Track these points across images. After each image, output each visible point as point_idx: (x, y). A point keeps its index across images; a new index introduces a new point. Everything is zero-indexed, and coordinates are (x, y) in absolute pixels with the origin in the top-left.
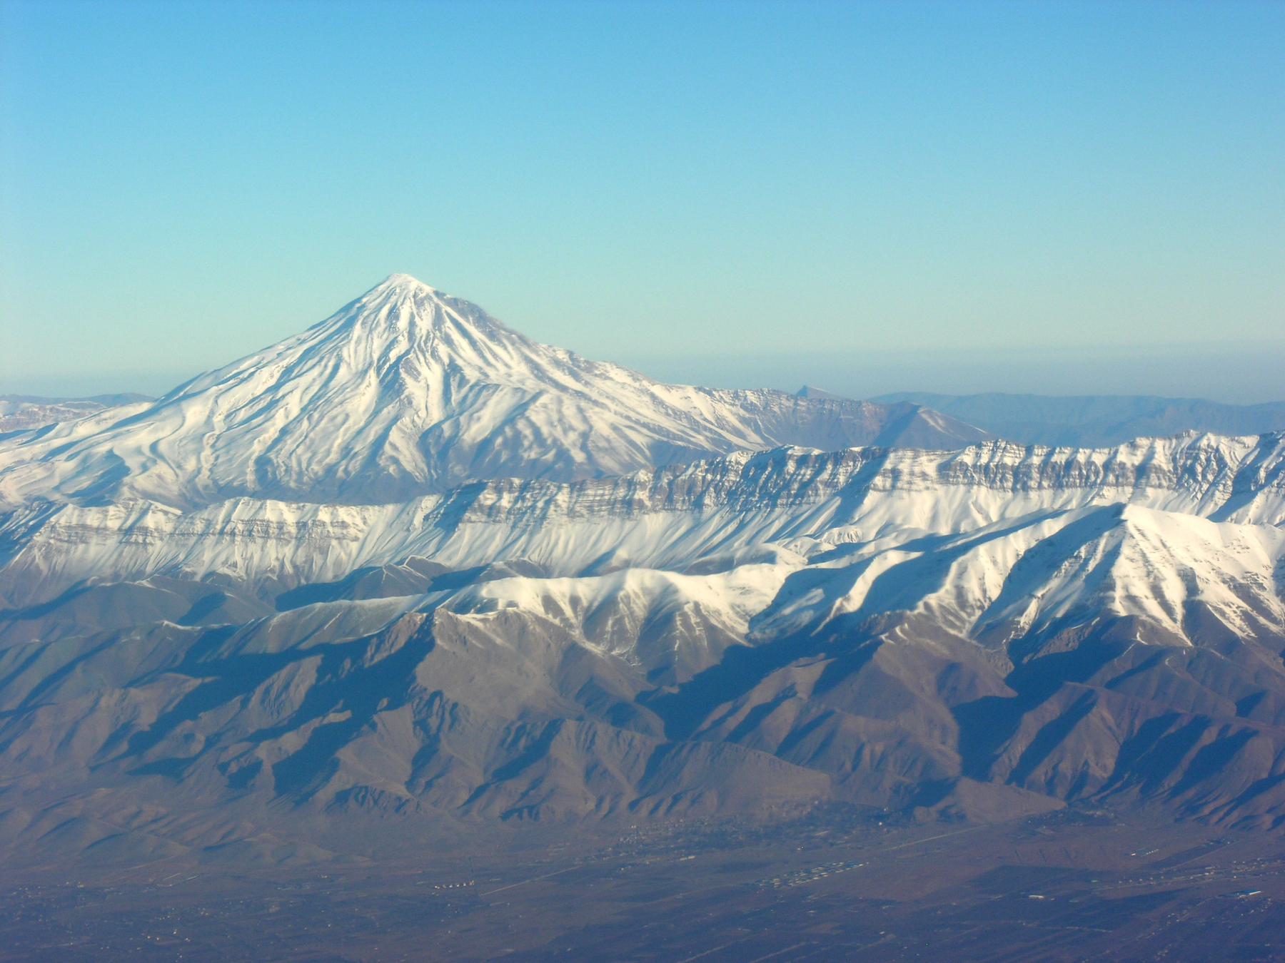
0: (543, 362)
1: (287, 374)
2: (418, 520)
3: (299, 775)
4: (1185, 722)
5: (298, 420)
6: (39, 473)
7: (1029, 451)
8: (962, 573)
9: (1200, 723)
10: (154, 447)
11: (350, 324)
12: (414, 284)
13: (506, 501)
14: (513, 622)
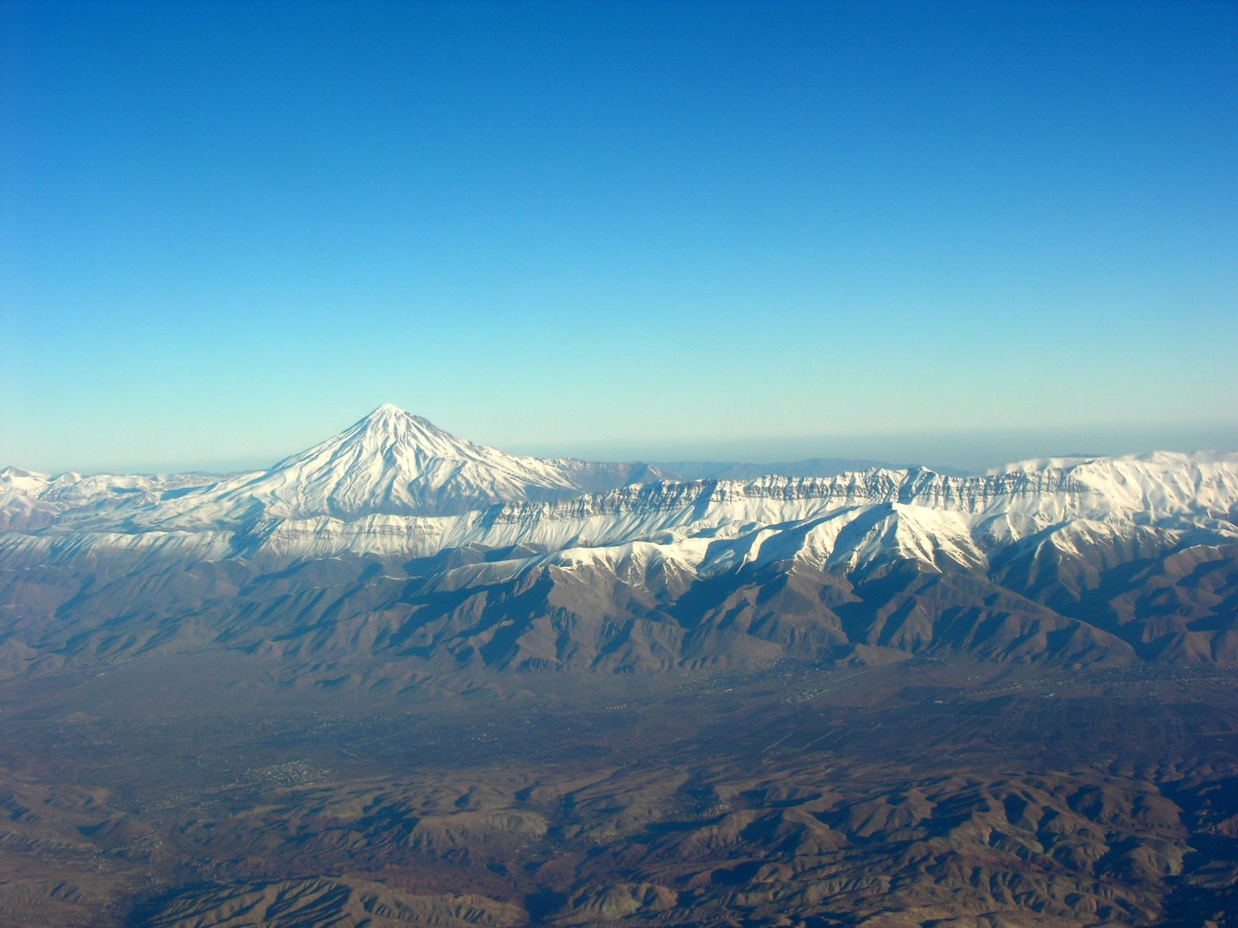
0: (462, 447)
1: (335, 455)
2: (469, 523)
3: (499, 651)
4: (966, 610)
5: (344, 478)
6: (215, 508)
7: (790, 480)
8: (812, 540)
9: (975, 611)
10: (273, 493)
11: (365, 429)
12: (394, 409)
13: (516, 512)
14: (582, 568)
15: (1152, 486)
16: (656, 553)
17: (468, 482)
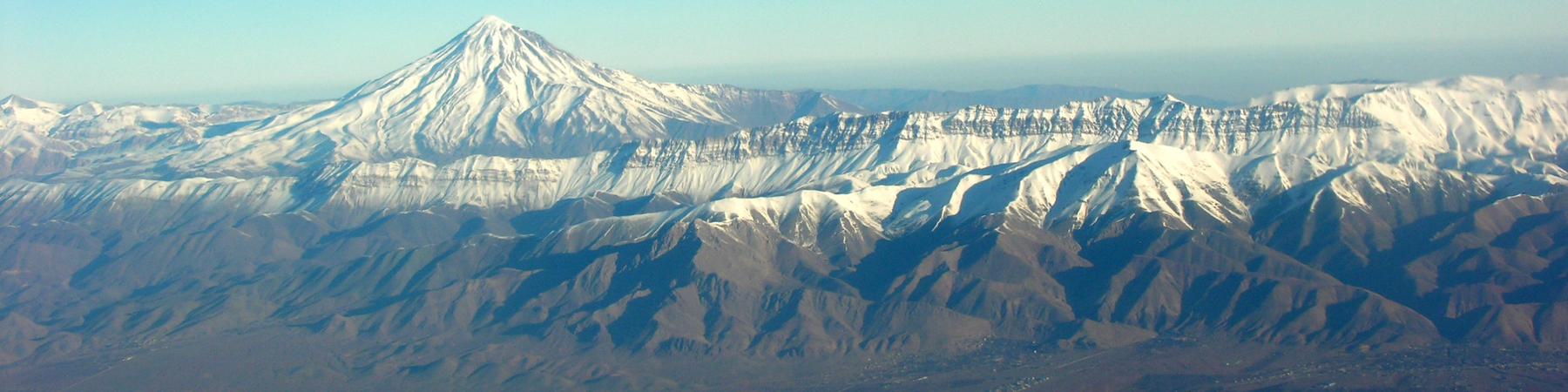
0: (585, 70)
1: (424, 81)
2: (595, 167)
4: (1224, 277)
5: (436, 109)
6: (272, 147)
7: (1001, 112)
8: (1028, 188)
9: (1235, 279)
10: (345, 128)
11: (462, 47)
12: (499, 22)
13: (654, 153)
14: (737, 224)
15: (1459, 120)
16: (830, 204)
17: (592, 114)
